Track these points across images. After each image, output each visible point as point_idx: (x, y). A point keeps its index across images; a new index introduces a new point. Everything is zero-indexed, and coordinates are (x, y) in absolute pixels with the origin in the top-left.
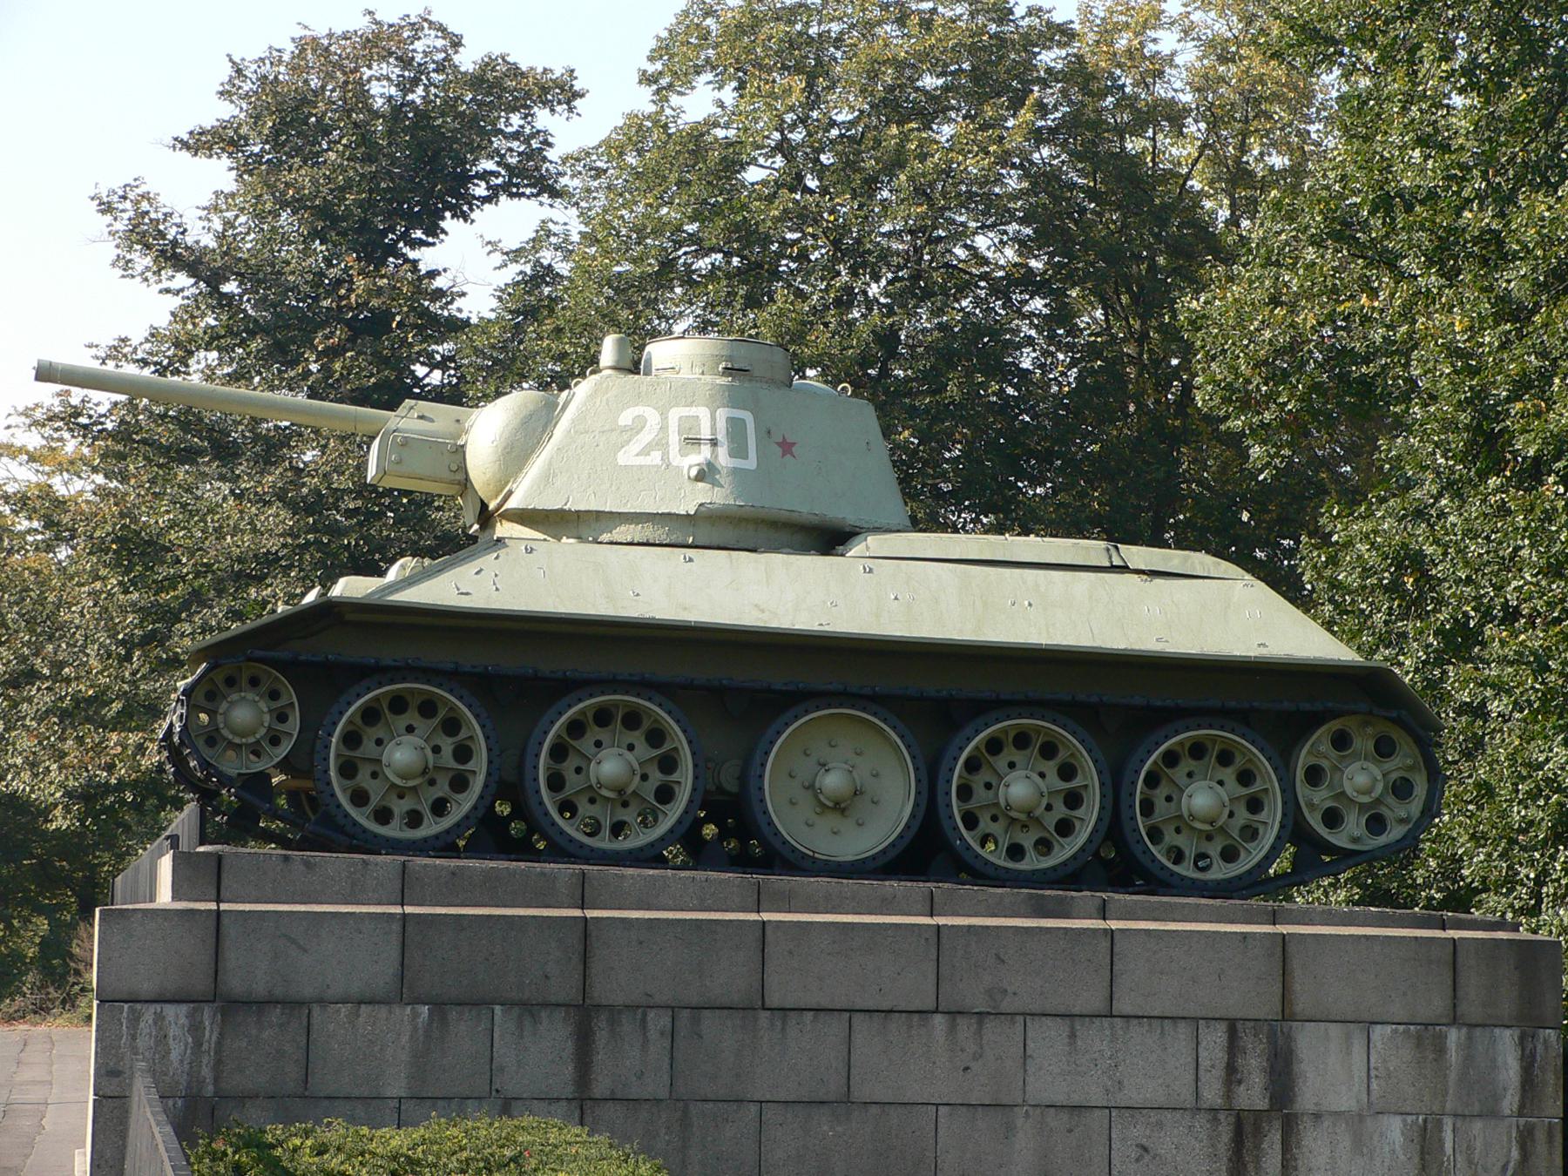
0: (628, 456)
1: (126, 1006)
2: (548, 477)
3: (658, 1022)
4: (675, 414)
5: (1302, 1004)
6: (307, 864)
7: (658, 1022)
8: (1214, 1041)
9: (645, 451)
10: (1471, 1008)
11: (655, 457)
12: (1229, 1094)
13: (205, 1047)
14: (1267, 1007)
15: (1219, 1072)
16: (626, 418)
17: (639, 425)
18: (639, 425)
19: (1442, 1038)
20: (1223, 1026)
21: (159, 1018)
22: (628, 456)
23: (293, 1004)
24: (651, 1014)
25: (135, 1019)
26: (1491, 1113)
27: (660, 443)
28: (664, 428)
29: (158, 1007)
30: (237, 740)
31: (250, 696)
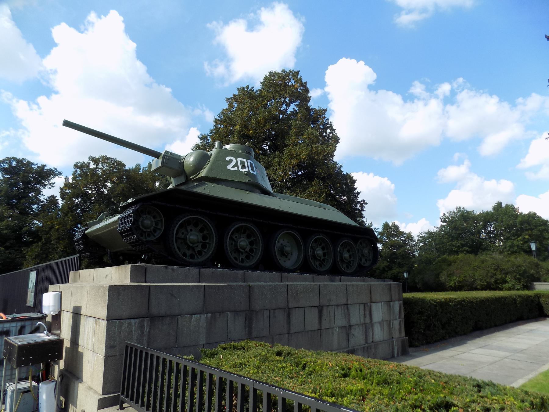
0: (230, 167)
1: (118, 321)
2: (211, 170)
3: (266, 313)
4: (239, 160)
5: (373, 300)
6: (173, 270)
7: (266, 313)
8: (362, 307)
9: (233, 167)
10: (393, 298)
11: (236, 169)
12: (364, 320)
13: (145, 333)
15: (363, 315)
16: (228, 159)
17: (231, 161)
18: (231, 161)
19: (390, 304)
20: (363, 305)
21: (130, 324)
22: (230, 167)
23: (173, 316)
24: (265, 312)
25: (121, 326)
26: (396, 319)
27: (236, 165)
28: (237, 162)
29: (129, 320)
30: (145, 230)
31: (149, 216)
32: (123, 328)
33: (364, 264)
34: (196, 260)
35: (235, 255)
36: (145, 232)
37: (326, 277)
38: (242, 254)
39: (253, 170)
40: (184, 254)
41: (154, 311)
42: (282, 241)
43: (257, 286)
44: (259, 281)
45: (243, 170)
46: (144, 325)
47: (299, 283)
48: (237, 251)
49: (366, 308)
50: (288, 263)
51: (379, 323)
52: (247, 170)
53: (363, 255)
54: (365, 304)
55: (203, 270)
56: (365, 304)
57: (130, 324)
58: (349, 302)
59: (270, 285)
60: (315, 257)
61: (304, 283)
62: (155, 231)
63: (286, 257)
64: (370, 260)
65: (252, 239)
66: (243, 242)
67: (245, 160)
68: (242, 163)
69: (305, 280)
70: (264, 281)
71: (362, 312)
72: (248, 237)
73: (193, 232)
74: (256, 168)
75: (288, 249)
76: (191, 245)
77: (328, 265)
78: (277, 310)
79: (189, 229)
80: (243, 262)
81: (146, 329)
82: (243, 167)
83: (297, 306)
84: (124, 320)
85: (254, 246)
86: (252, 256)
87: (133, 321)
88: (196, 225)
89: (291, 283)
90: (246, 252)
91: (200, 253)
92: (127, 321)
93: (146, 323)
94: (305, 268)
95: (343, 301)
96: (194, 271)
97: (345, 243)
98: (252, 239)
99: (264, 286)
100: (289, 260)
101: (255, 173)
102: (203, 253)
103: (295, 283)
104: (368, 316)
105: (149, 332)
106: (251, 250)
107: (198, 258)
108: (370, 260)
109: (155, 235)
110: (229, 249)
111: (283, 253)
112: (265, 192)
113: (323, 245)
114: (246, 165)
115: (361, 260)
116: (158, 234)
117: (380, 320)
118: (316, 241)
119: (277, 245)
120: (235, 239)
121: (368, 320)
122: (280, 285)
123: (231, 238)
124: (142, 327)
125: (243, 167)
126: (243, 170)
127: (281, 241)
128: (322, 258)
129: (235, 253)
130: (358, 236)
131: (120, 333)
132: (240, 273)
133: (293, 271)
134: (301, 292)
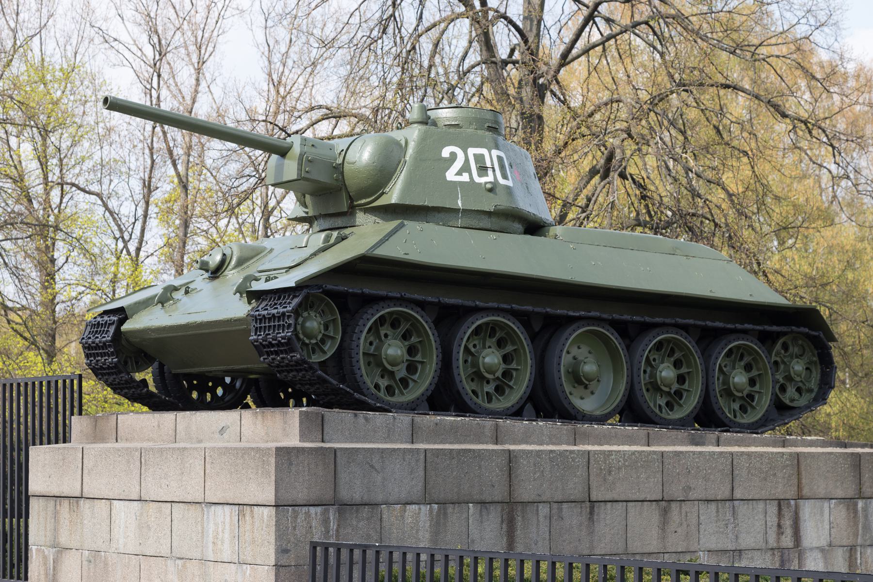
4: (472, 151)
11: (465, 177)
14: (791, 493)
15: (775, 529)
18: (453, 157)
27: (466, 168)
28: (467, 160)
32: (299, 520)
33: (792, 400)
34: (397, 399)
35: (474, 386)
36: (307, 345)
37: (682, 434)
38: (488, 382)
39: (505, 177)
40: (377, 387)
41: (345, 494)
42: (575, 352)
43: (523, 451)
44: (527, 443)
45: (483, 180)
46: (329, 518)
47: (615, 448)
48: (478, 376)
49: (785, 511)
50: (586, 404)
51: (822, 550)
52: (490, 178)
53: (789, 378)
54: (780, 503)
55: (419, 419)
56: (780, 503)
57: (308, 514)
58: (738, 494)
59: (551, 451)
60: (655, 387)
61: (626, 448)
62: (323, 341)
63: (586, 387)
64: (810, 391)
65: (509, 348)
66: (491, 358)
67: (484, 151)
68: (479, 158)
69: (631, 441)
70: (538, 441)
71: (773, 520)
72: (500, 344)
73: (390, 341)
74: (511, 166)
75: (589, 368)
76: (389, 367)
77: (691, 403)
78: (565, 506)
79: (382, 333)
80: (490, 400)
81: (333, 525)
82: (483, 170)
83: (608, 498)
84: (300, 508)
85: (514, 365)
86: (511, 387)
87: (312, 510)
88: (394, 325)
89: (597, 448)
90: (498, 378)
91: (404, 382)
92: (305, 509)
93: (332, 513)
94: (633, 412)
95: (723, 492)
96: (404, 419)
97: (738, 347)
98: (509, 348)
99: (539, 453)
100: (592, 393)
101: (510, 183)
102: (411, 384)
103: (606, 448)
104: (789, 532)
105: (337, 531)
106: (507, 374)
107: (403, 394)
108: (810, 391)
109: (326, 349)
110: (462, 373)
111: (579, 380)
112: (535, 228)
113: (677, 355)
114: (488, 164)
115: (783, 389)
116: (330, 349)
117: (823, 542)
118: (659, 346)
119: (566, 359)
120: (473, 350)
121: (787, 541)
122: (572, 452)
123: (467, 350)
124: (326, 521)
125: (483, 170)
126: (483, 180)
127: (575, 351)
128: (675, 386)
129: (472, 380)
130: (775, 328)
131: (294, 528)
132: (488, 423)
133: (601, 420)
134: (619, 468)
